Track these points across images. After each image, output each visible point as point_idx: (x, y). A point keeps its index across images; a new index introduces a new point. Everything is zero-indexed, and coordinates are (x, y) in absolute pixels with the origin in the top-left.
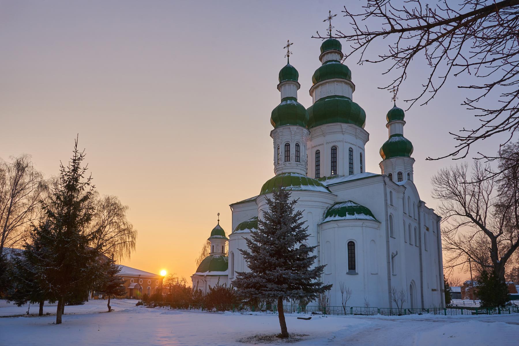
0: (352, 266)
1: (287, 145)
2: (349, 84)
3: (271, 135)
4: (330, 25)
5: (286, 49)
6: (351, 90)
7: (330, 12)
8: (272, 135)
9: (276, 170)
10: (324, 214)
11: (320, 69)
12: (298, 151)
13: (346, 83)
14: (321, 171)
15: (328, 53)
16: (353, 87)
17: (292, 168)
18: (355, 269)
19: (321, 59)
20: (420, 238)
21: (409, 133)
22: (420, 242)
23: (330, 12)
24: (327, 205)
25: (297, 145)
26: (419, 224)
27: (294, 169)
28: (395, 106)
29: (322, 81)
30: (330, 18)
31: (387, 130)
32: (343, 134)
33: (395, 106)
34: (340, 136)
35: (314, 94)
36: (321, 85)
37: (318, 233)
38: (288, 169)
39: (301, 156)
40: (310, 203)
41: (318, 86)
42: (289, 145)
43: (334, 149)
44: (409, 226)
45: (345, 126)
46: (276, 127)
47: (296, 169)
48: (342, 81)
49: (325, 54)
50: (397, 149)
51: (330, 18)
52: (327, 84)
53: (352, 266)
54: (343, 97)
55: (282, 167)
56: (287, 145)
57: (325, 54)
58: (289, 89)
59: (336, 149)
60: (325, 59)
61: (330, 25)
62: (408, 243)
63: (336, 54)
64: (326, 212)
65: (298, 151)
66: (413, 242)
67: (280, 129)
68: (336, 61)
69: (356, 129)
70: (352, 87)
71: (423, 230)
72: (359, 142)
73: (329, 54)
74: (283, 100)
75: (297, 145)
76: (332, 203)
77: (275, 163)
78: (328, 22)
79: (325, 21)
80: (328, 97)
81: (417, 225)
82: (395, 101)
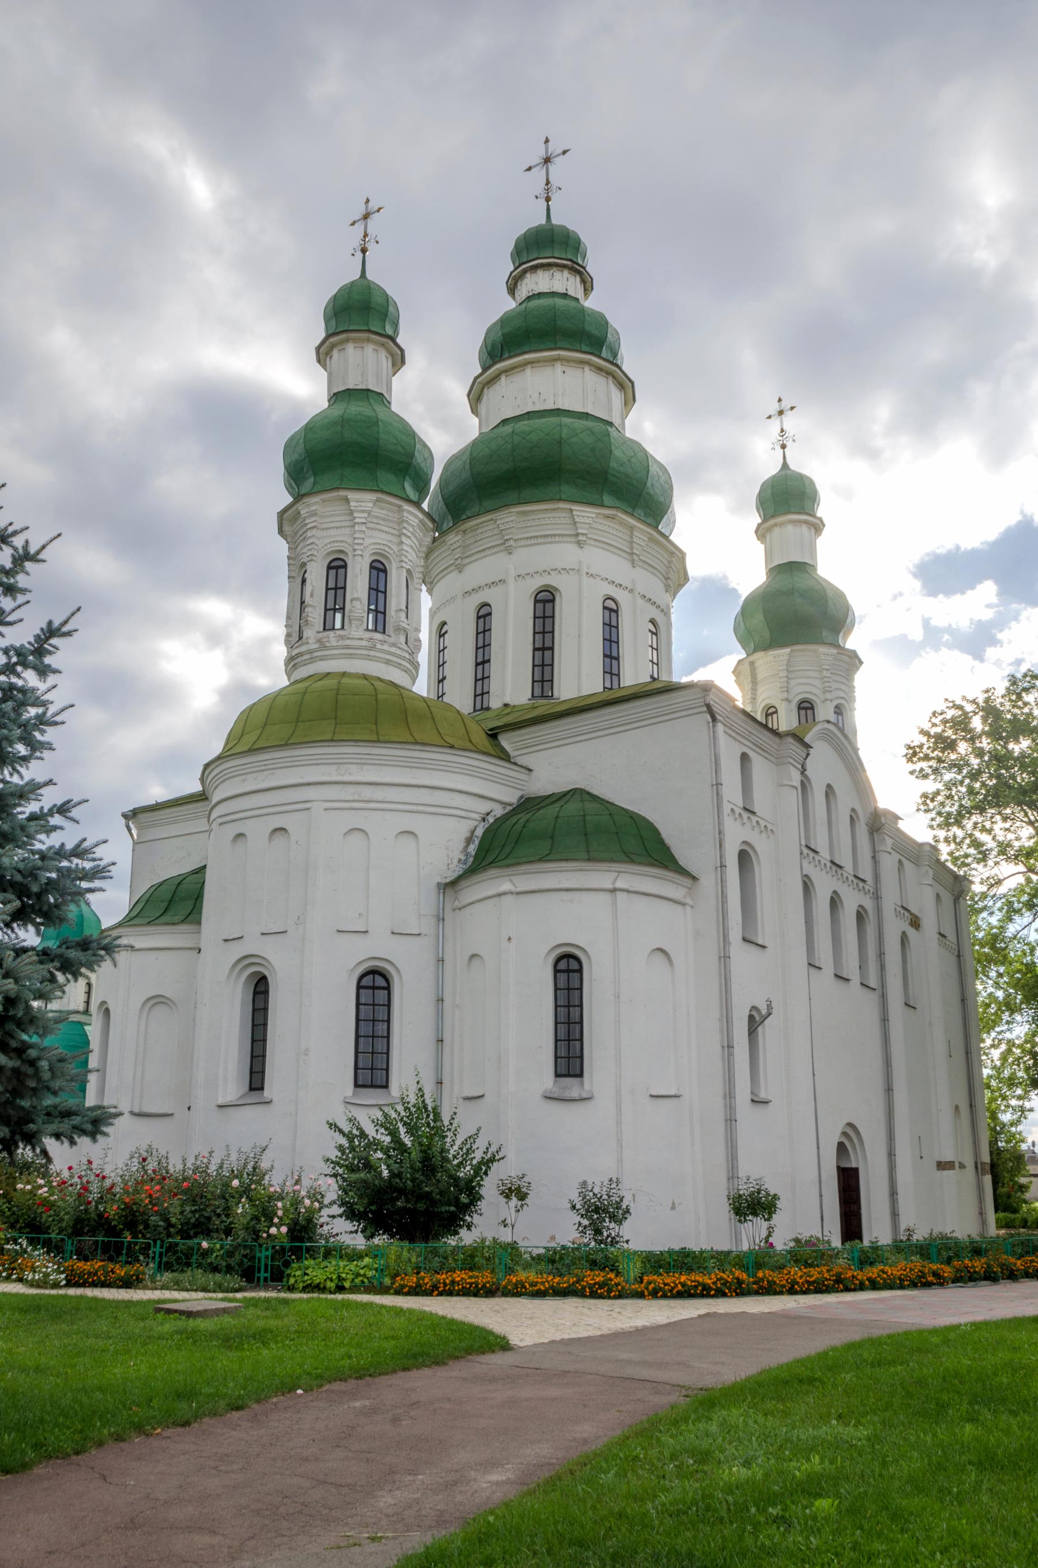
0: (570, 1059)
1: (337, 566)
2: (608, 373)
3: (281, 531)
4: (548, 183)
5: (360, 228)
6: (617, 397)
7: (547, 141)
8: (287, 528)
9: (292, 663)
10: (469, 841)
11: (504, 321)
12: (378, 590)
13: (599, 369)
14: (494, 685)
15: (535, 268)
16: (626, 386)
17: (351, 656)
18: (580, 1075)
19: (512, 290)
20: (881, 955)
21: (835, 563)
22: (882, 968)
23: (547, 141)
24: (484, 807)
25: (379, 569)
26: (877, 897)
27: (355, 655)
28: (785, 465)
29: (510, 357)
30: (547, 160)
31: (760, 548)
32: (579, 543)
33: (785, 465)
34: (566, 553)
35: (483, 407)
36: (506, 371)
37: (440, 919)
38: (333, 657)
39: (391, 611)
40: (408, 795)
41: (496, 378)
42: (345, 567)
43: (545, 602)
44: (835, 902)
45: (586, 515)
46: (298, 498)
47: (368, 658)
48: (583, 362)
49: (525, 272)
50: (797, 615)
51: (547, 160)
52: (528, 371)
53: (570, 1059)
54: (586, 416)
55: (310, 652)
56: (337, 566)
57: (525, 272)
58: (362, 363)
59: (553, 601)
60: (525, 288)
61: (548, 183)
62: (829, 970)
63: (566, 273)
64: (480, 832)
65: (378, 590)
66: (851, 967)
67: (314, 504)
68: (565, 296)
69: (632, 528)
70: (621, 386)
71: (894, 927)
72: (649, 583)
73: (540, 273)
74: (336, 397)
75: (379, 569)
76: (512, 797)
77: (288, 635)
78: (539, 174)
79: (529, 169)
80: (529, 415)
81: (868, 904)
82: (783, 447)
